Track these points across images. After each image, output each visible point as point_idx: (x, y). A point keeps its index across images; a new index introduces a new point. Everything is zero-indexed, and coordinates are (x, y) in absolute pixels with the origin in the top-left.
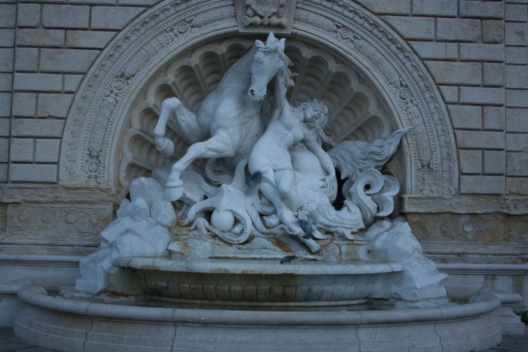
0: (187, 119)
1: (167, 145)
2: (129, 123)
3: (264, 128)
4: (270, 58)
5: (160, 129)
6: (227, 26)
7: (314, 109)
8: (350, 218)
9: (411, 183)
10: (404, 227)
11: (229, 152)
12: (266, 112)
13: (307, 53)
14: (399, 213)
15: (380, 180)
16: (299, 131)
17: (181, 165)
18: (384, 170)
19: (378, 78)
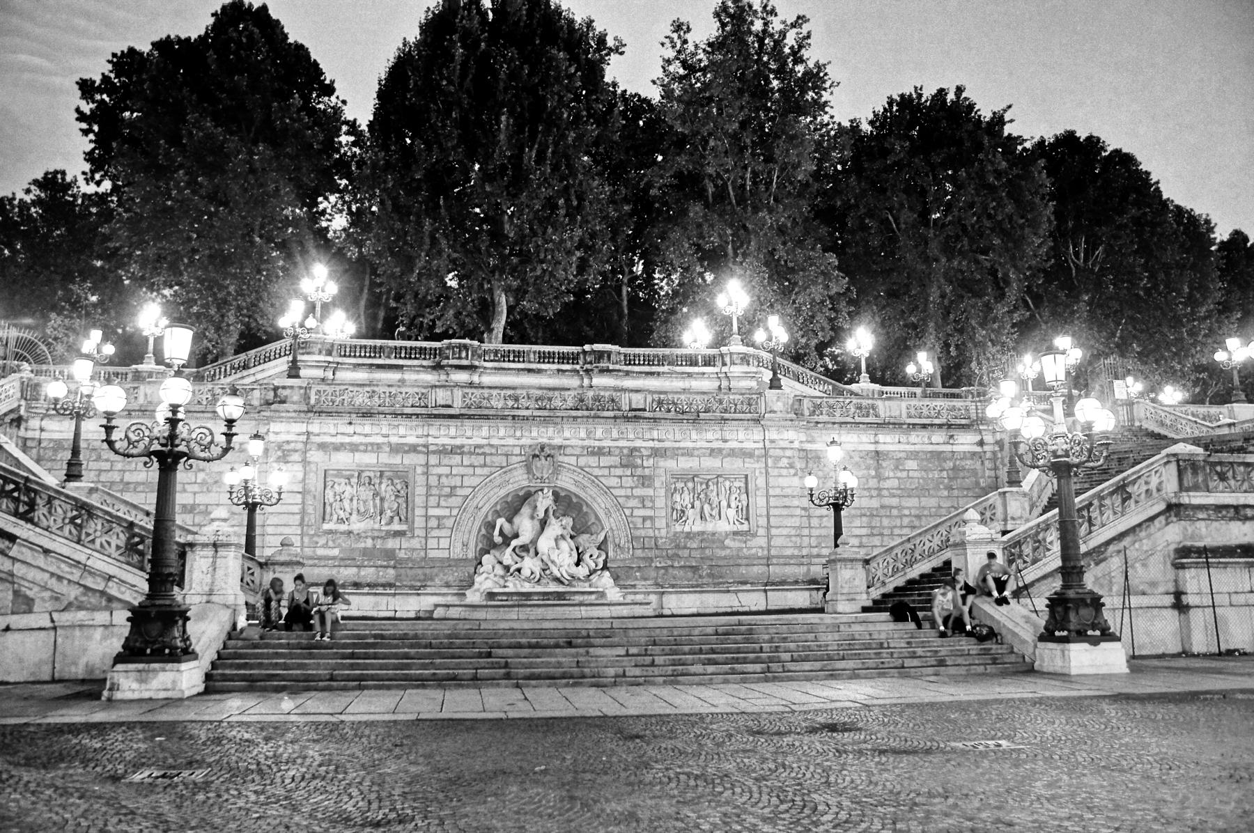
0: (507, 527)
1: (498, 539)
2: (480, 530)
3: (543, 529)
4: (544, 502)
5: (496, 532)
6: (526, 483)
7: (568, 521)
9: (611, 554)
10: (607, 574)
11: (527, 542)
13: (563, 494)
14: (605, 567)
15: (596, 553)
16: (559, 532)
17: (510, 549)
18: (599, 548)
19: (595, 506)
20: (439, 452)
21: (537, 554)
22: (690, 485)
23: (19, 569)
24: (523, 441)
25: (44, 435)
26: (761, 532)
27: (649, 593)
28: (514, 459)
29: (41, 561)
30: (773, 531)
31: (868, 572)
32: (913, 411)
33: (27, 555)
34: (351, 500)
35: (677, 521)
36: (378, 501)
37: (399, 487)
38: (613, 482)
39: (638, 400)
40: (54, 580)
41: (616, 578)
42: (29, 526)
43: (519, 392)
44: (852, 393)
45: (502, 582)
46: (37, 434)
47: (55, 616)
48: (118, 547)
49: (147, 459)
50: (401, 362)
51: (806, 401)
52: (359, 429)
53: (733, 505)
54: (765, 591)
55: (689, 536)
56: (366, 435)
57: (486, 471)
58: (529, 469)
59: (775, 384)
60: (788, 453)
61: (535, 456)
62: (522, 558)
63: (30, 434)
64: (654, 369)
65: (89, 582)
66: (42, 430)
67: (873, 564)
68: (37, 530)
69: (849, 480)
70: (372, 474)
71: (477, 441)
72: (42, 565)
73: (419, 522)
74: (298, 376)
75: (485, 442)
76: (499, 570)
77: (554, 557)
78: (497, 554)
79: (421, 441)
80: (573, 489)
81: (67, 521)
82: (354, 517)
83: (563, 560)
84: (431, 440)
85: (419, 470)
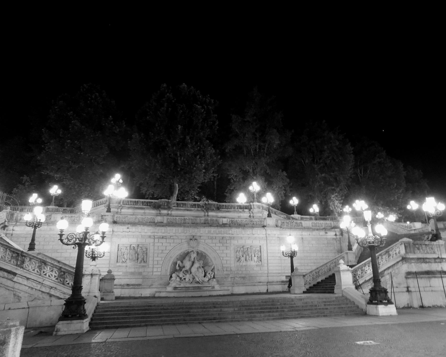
1: (177, 268)
5: (177, 266)
6: (187, 249)
8: (206, 279)
9: (216, 273)
10: (215, 280)
12: (193, 263)
14: (214, 277)
15: (211, 272)
19: (210, 256)
20: (159, 238)
21: (191, 273)
22: (242, 249)
23: (17, 286)
24: (187, 234)
25: (14, 232)
26: (266, 265)
27: (228, 286)
28: (183, 241)
29: (25, 282)
30: (269, 265)
31: (305, 279)
32: (313, 224)
33: (20, 280)
34: (127, 255)
35: (238, 261)
36: (136, 255)
37: (144, 250)
38: (217, 248)
39: (225, 221)
40: (30, 289)
41: (218, 281)
42: (22, 269)
43: (185, 218)
44: (293, 218)
45: (179, 283)
46: (11, 232)
47: (29, 303)
48: (55, 277)
49: (74, 246)
50: (144, 207)
51: (279, 221)
52: (131, 230)
53: (256, 256)
54: (267, 285)
55: (242, 266)
56: (133, 232)
57: (174, 245)
58: (189, 244)
59: (269, 216)
60: (274, 238)
61: (191, 239)
62: (186, 274)
63: (8, 232)
64: (229, 210)
65: (43, 289)
66: (13, 230)
67: (306, 277)
68: (25, 271)
69: (295, 248)
70: (135, 246)
71: (172, 234)
72: (26, 284)
73: (151, 262)
74: (110, 212)
75: (174, 234)
76: (178, 279)
77: (197, 274)
78: (177, 274)
79: (153, 234)
80: (203, 251)
81: (36, 267)
82: (128, 261)
83: (200, 276)
84: (156, 234)
85: (151, 244)
